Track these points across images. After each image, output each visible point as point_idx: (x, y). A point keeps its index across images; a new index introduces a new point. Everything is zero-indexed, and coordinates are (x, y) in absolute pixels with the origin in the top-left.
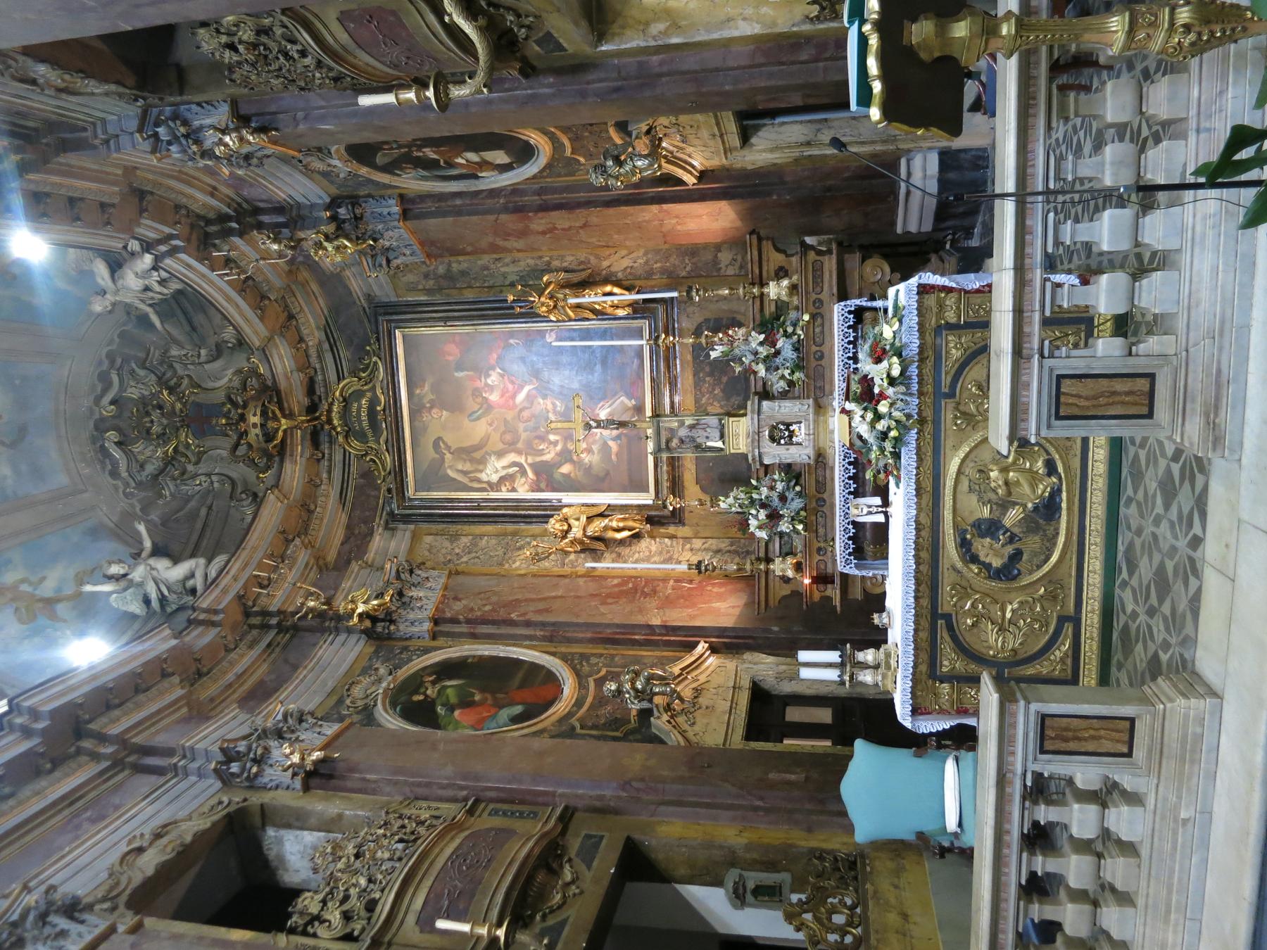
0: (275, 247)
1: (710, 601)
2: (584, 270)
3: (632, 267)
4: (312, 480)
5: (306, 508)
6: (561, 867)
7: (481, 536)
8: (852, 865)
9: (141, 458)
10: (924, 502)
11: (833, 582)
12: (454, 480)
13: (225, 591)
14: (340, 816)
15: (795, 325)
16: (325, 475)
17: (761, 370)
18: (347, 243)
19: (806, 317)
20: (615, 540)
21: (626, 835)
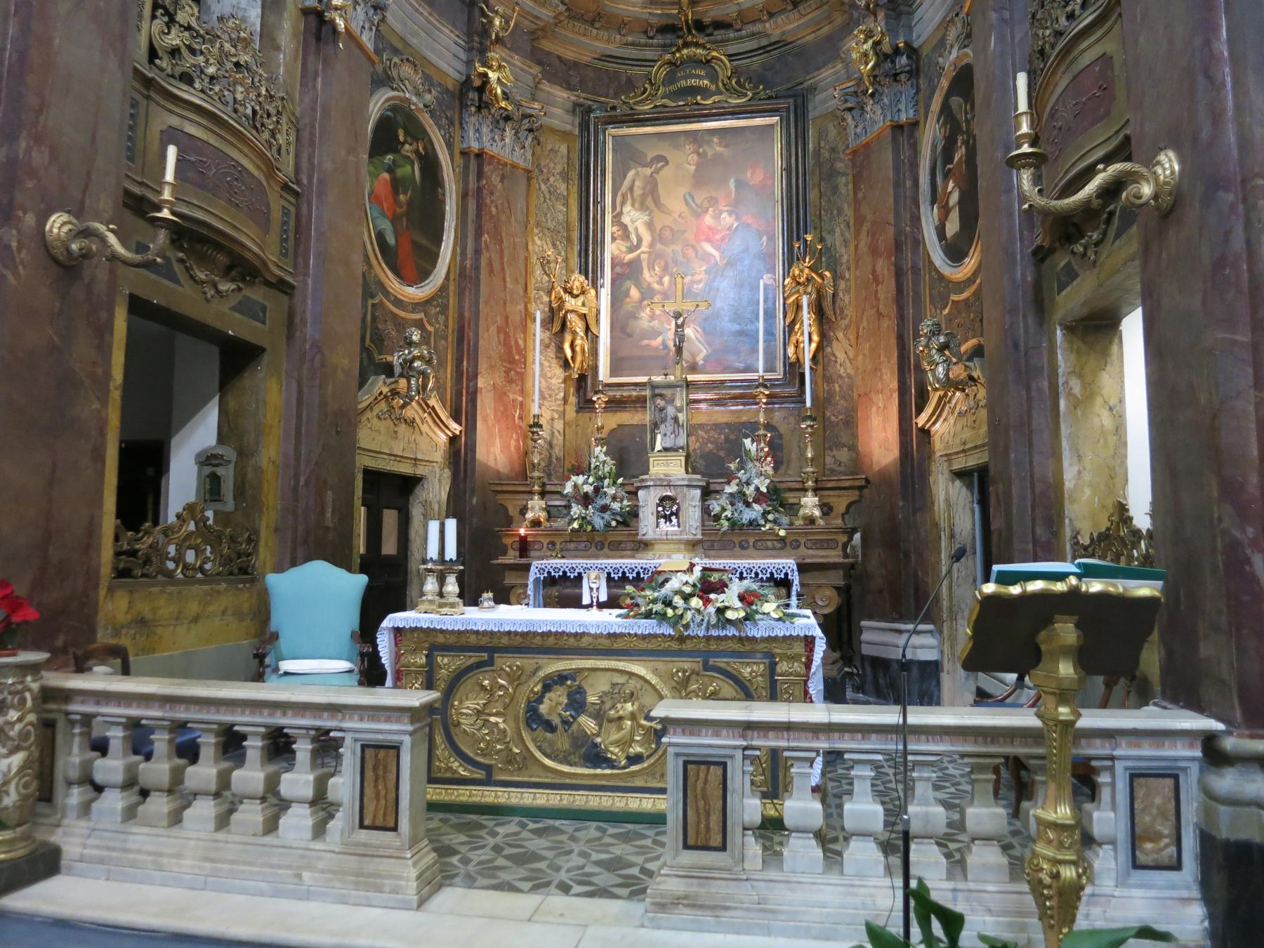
1: (501, 437)
2: (835, 314)
3: (836, 362)
4: (625, 24)
6: (233, 280)
7: (567, 205)
8: (244, 571)
10: (603, 641)
11: (521, 556)
12: (625, 177)
14: (278, 48)
15: (775, 521)
16: (630, 39)
17: (731, 489)
19: (782, 533)
20: (562, 342)
21: (266, 346)
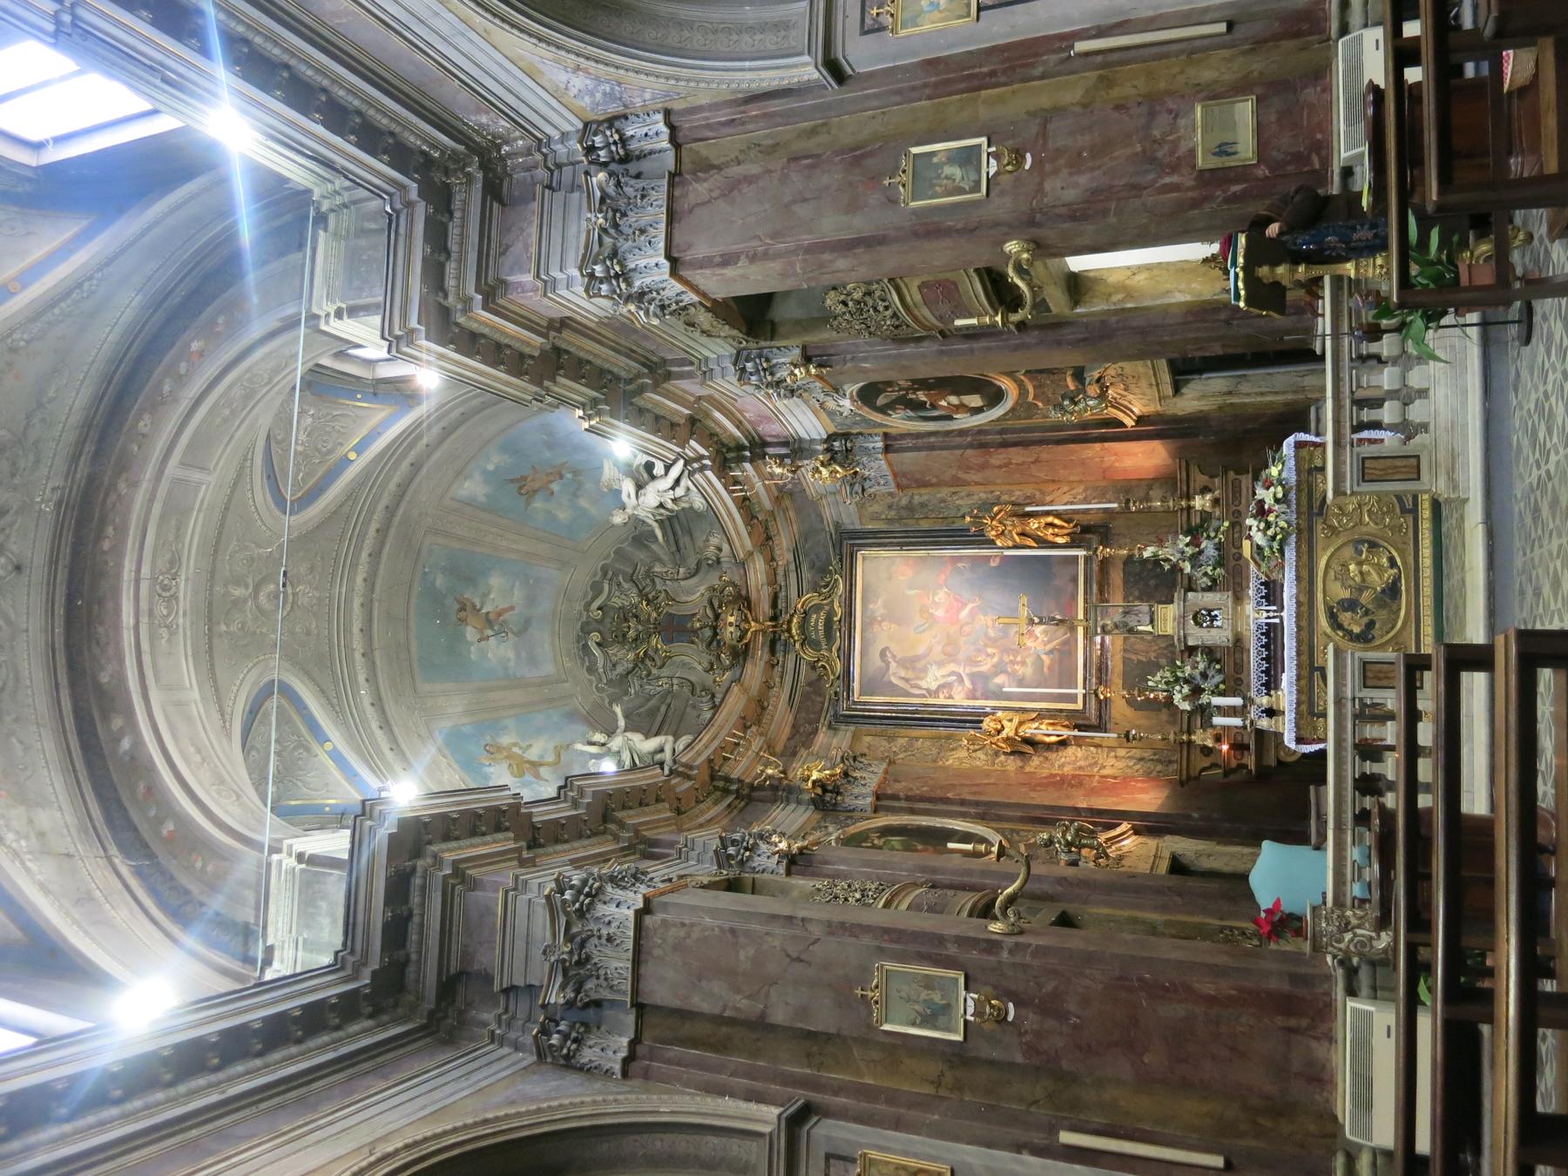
0: (778, 470)
5: (760, 706)
7: (917, 739)
9: (614, 659)
13: (699, 754)
16: (778, 680)
17: (1187, 567)
18: (838, 468)
